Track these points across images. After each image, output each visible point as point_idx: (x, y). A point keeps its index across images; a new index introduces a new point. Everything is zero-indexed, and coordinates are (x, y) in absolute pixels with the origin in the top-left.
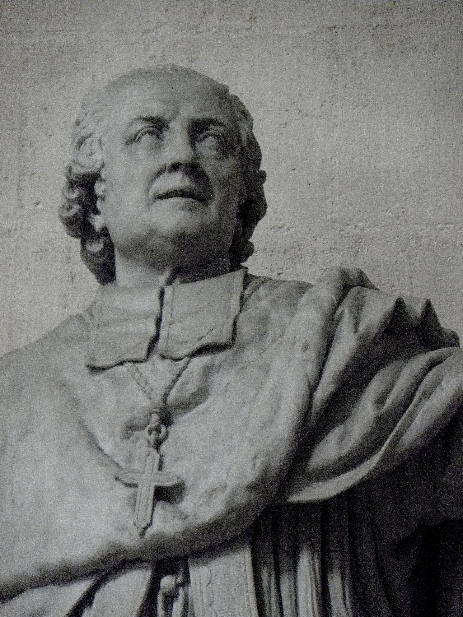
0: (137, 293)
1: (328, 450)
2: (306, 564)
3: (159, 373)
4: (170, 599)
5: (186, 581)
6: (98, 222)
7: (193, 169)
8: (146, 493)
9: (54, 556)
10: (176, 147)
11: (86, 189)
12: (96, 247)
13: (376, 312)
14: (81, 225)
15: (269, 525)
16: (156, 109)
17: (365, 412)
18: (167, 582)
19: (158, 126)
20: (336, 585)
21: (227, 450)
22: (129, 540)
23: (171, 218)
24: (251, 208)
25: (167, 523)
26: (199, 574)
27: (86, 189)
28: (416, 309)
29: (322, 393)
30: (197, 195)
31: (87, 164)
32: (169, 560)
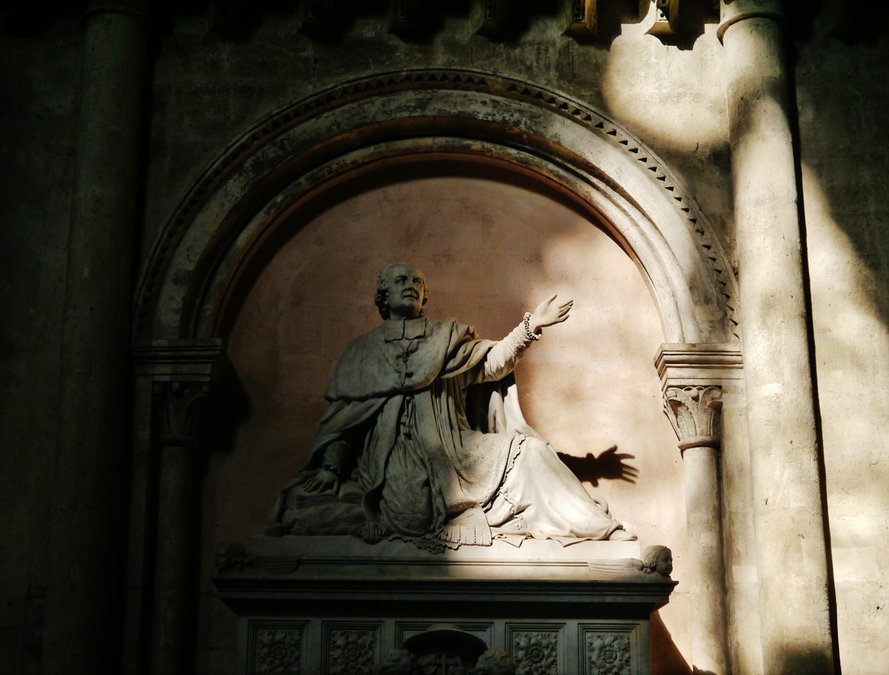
1: (451, 364)
2: (444, 395)
4: (409, 402)
5: (413, 398)
8: (403, 374)
9: (377, 390)
16: (403, 273)
17: (460, 355)
18: (408, 398)
20: (451, 400)
26: (417, 397)
31: (383, 287)
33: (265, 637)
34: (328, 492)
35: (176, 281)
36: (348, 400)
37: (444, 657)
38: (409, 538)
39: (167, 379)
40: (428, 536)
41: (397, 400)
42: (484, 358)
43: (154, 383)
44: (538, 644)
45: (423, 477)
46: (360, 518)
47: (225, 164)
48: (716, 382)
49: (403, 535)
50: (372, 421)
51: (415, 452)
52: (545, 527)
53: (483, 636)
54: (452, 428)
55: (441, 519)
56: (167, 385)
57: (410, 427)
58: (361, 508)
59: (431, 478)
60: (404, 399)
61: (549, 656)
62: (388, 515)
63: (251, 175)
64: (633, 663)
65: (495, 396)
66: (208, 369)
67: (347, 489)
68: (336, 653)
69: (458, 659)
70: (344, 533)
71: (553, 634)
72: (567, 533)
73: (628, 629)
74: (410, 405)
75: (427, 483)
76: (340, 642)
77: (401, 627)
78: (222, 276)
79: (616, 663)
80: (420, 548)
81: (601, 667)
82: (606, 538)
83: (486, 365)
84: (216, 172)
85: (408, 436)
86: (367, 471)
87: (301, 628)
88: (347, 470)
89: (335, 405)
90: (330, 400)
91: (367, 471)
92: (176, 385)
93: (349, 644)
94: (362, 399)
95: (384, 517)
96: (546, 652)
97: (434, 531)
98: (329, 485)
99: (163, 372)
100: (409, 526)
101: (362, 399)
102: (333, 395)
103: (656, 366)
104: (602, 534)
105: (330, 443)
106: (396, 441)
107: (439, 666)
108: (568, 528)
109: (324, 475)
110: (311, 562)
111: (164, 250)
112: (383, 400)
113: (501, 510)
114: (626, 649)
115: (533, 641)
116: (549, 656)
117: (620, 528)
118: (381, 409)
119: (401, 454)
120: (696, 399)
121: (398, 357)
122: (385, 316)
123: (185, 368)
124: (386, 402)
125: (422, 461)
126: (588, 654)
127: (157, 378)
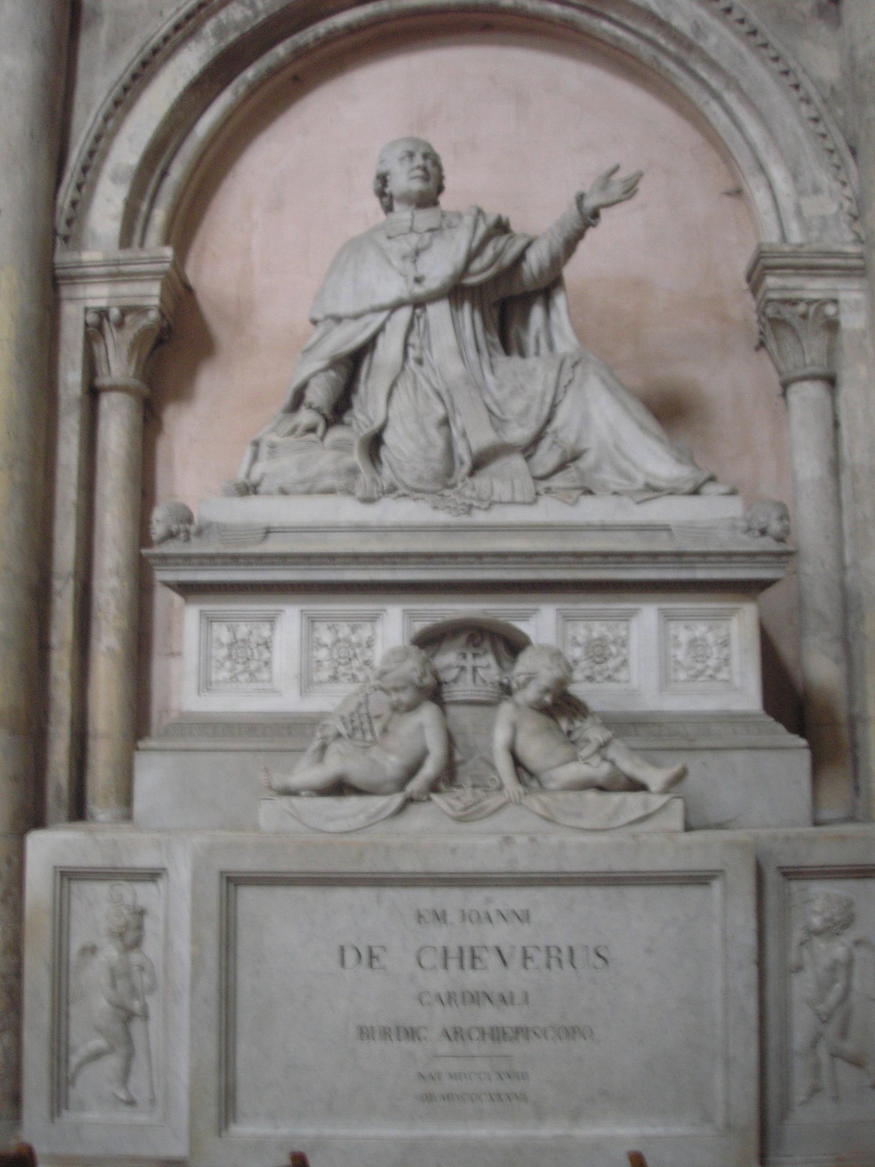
0: (403, 214)
1: (477, 265)
2: (467, 307)
3: (414, 239)
4: (419, 318)
5: (425, 310)
6: (387, 190)
7: (425, 169)
10: (419, 161)
11: (383, 179)
12: (386, 200)
13: (491, 219)
14: (381, 193)
15: (456, 292)
16: (410, 148)
17: (489, 252)
18: (418, 311)
19: (411, 155)
21: (440, 265)
22: (405, 295)
23: (417, 186)
24: (440, 189)
25: (419, 290)
27: (383, 179)
28: (504, 220)
29: (475, 244)
30: (426, 178)
31: (383, 169)
32: (419, 304)
33: (222, 633)
34: (311, 436)
35: (115, 179)
36: (338, 319)
37: (469, 656)
38: (420, 495)
39: (102, 303)
40: (447, 492)
41: (404, 314)
42: (521, 257)
43: (86, 310)
44: (601, 639)
45: (440, 411)
46: (353, 471)
47: (177, 27)
48: (832, 295)
49: (414, 493)
50: (368, 347)
51: (428, 381)
52: (608, 476)
53: (523, 627)
54: (478, 350)
55: (466, 469)
56: (103, 313)
57: (422, 348)
58: (356, 458)
59: (451, 415)
60: (413, 314)
61: (619, 654)
62: (391, 466)
63: (212, 41)
64: (735, 661)
65: (537, 314)
66: (155, 288)
67: (337, 434)
68: (323, 654)
69: (490, 659)
70: (330, 491)
71: (623, 625)
72: (639, 485)
73: (725, 616)
74: (422, 322)
75: (446, 422)
76: (327, 637)
77: (410, 616)
78: (177, 171)
79: (712, 662)
80: (435, 508)
81: (691, 668)
82: (696, 492)
83: (525, 267)
84: (166, 39)
85: (420, 362)
86: (364, 412)
87: (271, 620)
88: (339, 409)
89: (321, 329)
90: (315, 322)
91: (364, 412)
92: (115, 313)
93: (338, 640)
94: (356, 317)
95: (386, 471)
96: (614, 649)
97: (454, 486)
98: (312, 430)
99: (98, 295)
100: (420, 479)
101: (356, 317)
102: (319, 316)
103: (749, 278)
104: (689, 486)
105: (314, 375)
106: (403, 368)
107: (463, 669)
108: (641, 480)
109: (305, 417)
110: (284, 530)
111: (98, 139)
112: (383, 316)
113: (547, 457)
114: (725, 644)
115: (595, 635)
116: (619, 654)
117: (712, 479)
118: (382, 329)
119: (409, 385)
120: (804, 316)
121: (404, 258)
122: (388, 209)
123: (125, 289)
124: (388, 318)
125: (439, 395)
126: (672, 651)
127: (91, 304)
